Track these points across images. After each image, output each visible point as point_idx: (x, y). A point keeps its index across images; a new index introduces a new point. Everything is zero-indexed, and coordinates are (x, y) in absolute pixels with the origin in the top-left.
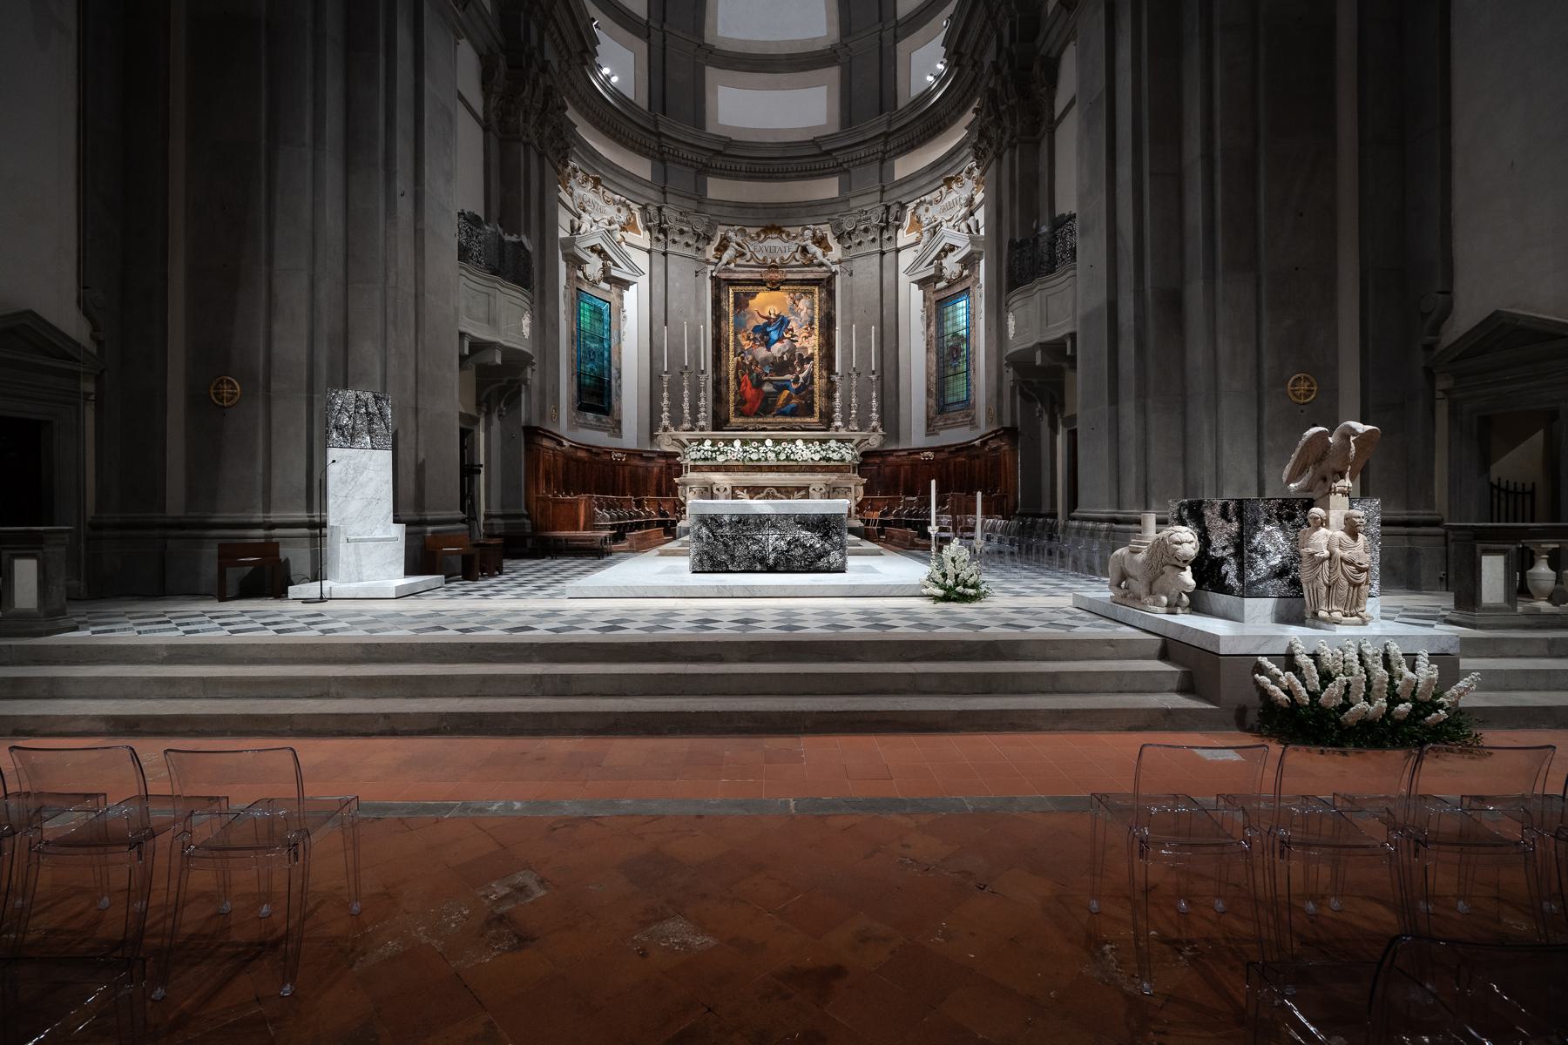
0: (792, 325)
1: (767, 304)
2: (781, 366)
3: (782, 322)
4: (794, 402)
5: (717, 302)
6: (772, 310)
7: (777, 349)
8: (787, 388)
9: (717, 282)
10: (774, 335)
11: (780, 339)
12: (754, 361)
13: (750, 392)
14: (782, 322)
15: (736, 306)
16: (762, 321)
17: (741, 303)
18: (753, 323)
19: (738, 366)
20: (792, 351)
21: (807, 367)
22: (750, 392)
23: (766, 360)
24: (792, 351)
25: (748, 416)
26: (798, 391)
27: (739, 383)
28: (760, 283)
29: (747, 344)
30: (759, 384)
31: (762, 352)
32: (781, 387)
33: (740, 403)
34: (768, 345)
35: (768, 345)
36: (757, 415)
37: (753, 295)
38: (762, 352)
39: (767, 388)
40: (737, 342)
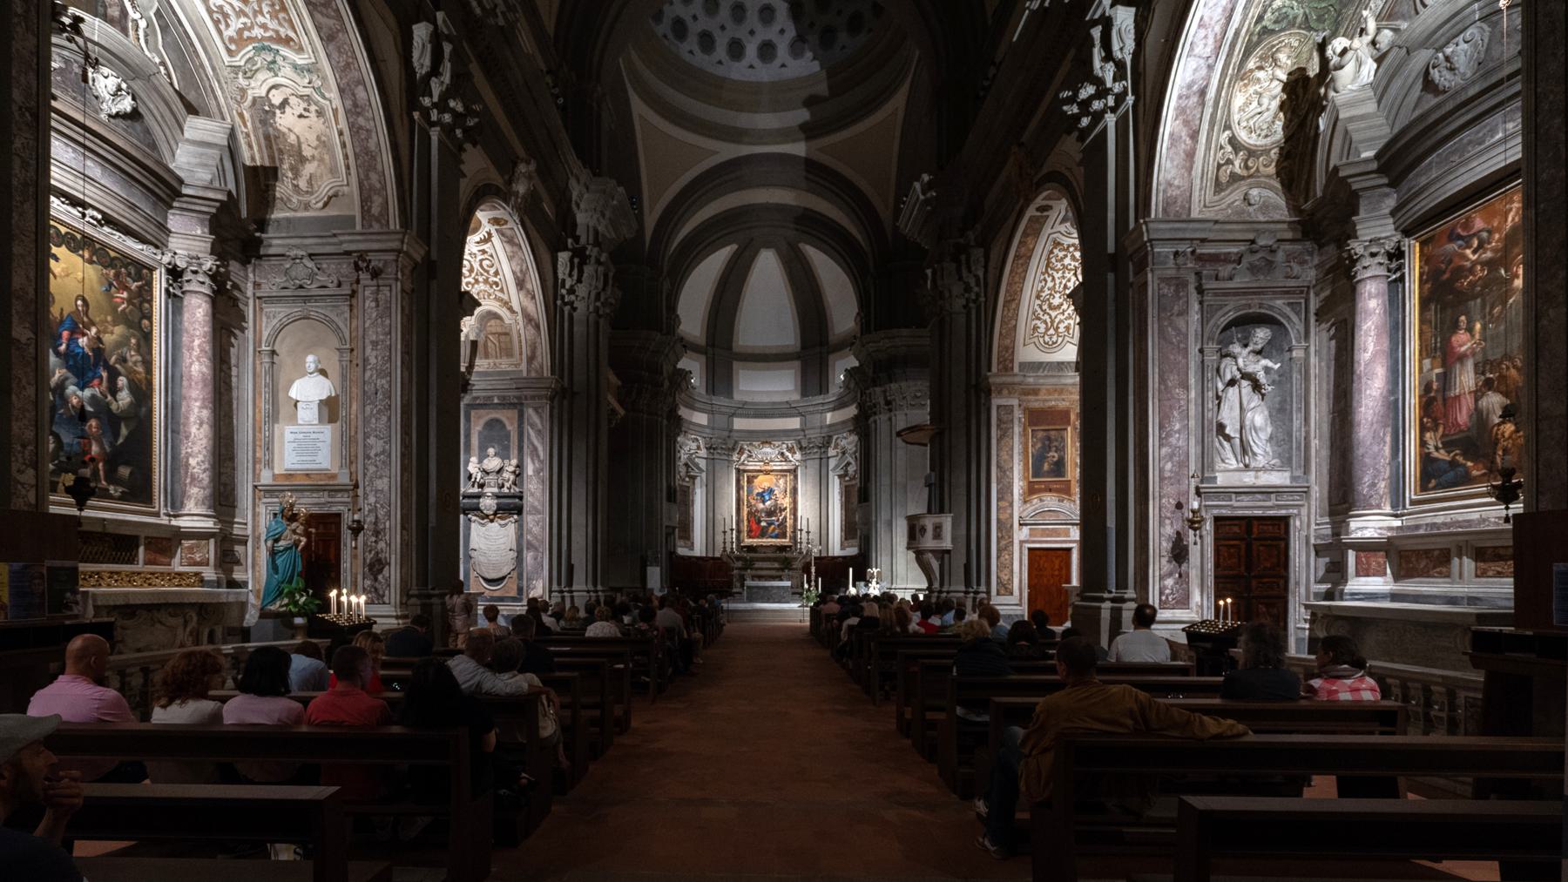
0: (776, 492)
1: (763, 481)
2: (770, 513)
3: (771, 491)
4: (777, 532)
5: (738, 481)
6: (766, 485)
7: (768, 503)
8: (773, 524)
9: (738, 471)
10: (767, 498)
11: (770, 499)
12: (757, 511)
13: (755, 526)
14: (771, 491)
15: (748, 482)
16: (761, 490)
17: (750, 481)
18: (756, 491)
19: (749, 513)
20: (776, 505)
21: (784, 513)
22: (755, 526)
23: (762, 510)
24: (776, 505)
25: (753, 538)
26: (779, 526)
27: (749, 521)
28: (760, 471)
29: (753, 502)
30: (760, 521)
31: (761, 506)
32: (770, 524)
33: (750, 531)
34: (764, 502)
35: (764, 502)
36: (758, 537)
37: (756, 477)
38: (761, 506)
39: (763, 524)
40: (748, 501)
